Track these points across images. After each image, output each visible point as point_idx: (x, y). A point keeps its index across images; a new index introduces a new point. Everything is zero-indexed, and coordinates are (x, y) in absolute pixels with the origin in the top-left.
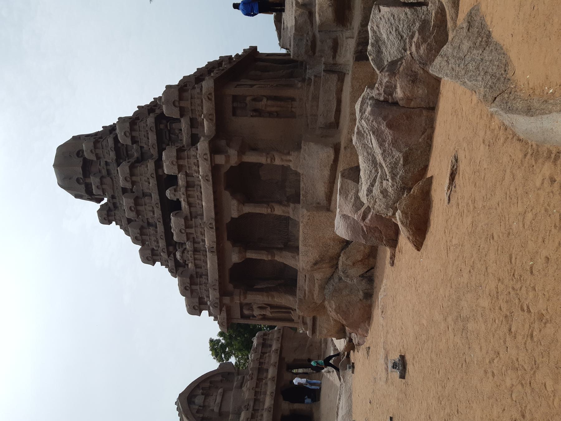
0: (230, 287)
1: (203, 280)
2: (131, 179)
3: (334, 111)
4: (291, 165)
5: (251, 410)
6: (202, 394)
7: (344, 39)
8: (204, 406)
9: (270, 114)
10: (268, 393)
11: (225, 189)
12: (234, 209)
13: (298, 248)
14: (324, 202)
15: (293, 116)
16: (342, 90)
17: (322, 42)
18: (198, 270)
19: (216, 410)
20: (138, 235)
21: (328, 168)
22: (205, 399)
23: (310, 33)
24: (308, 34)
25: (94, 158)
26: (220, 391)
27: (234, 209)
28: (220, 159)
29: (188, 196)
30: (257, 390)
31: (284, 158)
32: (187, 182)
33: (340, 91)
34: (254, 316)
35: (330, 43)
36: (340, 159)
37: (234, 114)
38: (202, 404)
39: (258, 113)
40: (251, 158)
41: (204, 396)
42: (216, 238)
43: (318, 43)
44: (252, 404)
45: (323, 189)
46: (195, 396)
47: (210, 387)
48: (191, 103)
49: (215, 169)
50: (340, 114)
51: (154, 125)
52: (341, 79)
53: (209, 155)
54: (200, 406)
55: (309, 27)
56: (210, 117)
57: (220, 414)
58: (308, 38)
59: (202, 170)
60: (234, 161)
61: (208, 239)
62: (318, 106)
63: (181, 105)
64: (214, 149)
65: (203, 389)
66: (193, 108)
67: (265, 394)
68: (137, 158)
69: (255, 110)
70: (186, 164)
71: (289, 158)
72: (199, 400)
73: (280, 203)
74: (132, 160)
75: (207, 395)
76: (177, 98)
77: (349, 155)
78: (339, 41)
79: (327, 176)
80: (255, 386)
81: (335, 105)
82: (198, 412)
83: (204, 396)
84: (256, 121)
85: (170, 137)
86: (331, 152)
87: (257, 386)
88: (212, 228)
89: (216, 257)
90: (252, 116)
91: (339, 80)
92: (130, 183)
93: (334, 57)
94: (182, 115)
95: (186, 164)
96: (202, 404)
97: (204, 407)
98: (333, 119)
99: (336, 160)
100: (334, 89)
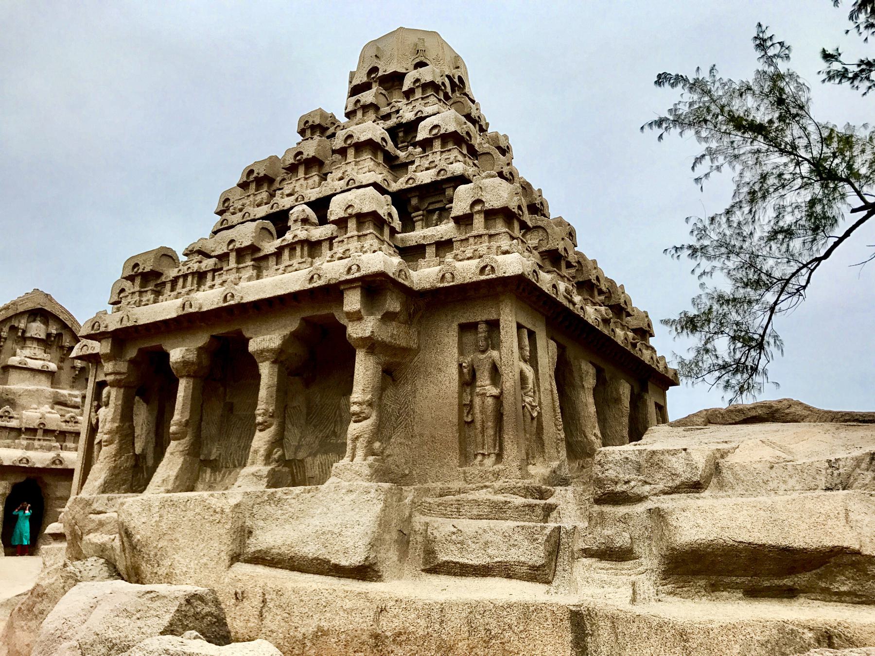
0: (132, 353)
1: (150, 296)
2: (350, 146)
3: (461, 561)
4: (346, 460)
6: (49, 335)
7: (633, 578)
10: (30, 454)
11: (303, 319)
12: (265, 340)
13: (192, 489)
14: (256, 544)
15: (465, 458)
16: (509, 577)
17: (625, 519)
18: (168, 286)
19: (14, 361)
20: (255, 175)
21: (323, 553)
22: (39, 340)
23: (647, 488)
24: (646, 483)
25: (405, 88)
26: (53, 366)
27: (265, 340)
28: (353, 301)
29: (292, 247)
30: (40, 432)
31: (361, 444)
33: (506, 571)
34: (99, 407)
35: (622, 540)
36: (343, 581)
37: (466, 328)
38: (28, 335)
39: (468, 380)
40: (364, 370)
41: (43, 336)
42: (208, 311)
43: (622, 510)
44: (14, 423)
45: (279, 542)
46: (46, 323)
47: (62, 347)
48: (480, 236)
49: (333, 292)
50: (455, 575)
51: (449, 175)
52: (538, 574)
53: (357, 275)
54: (24, 332)
55: (661, 486)
56: (448, 276)
57: (7, 368)
58: (632, 484)
59: (331, 268)
60: (356, 331)
62: (479, 517)
63: (476, 216)
64: (374, 286)
65: (59, 336)
66: (471, 240)
67: (27, 448)
68: (397, 157)
69: (473, 373)
70: (349, 235)
71: (360, 453)
72: (37, 329)
73: (278, 441)
74: (390, 146)
75: (46, 343)
76: (488, 206)
77: (348, 604)
78: (629, 564)
79: (306, 550)
80: (48, 427)
81: (475, 562)
82: (13, 329)
83: (43, 336)
85: (432, 212)
86: (355, 559)
87: (47, 432)
88: (225, 299)
89: (174, 315)
90: (460, 365)
91: (533, 568)
92: (343, 145)
93: (588, 553)
94: (458, 220)
95: (349, 235)
96: (28, 335)
97: (23, 339)
98: (443, 557)
99: (339, 571)
100: (513, 556)
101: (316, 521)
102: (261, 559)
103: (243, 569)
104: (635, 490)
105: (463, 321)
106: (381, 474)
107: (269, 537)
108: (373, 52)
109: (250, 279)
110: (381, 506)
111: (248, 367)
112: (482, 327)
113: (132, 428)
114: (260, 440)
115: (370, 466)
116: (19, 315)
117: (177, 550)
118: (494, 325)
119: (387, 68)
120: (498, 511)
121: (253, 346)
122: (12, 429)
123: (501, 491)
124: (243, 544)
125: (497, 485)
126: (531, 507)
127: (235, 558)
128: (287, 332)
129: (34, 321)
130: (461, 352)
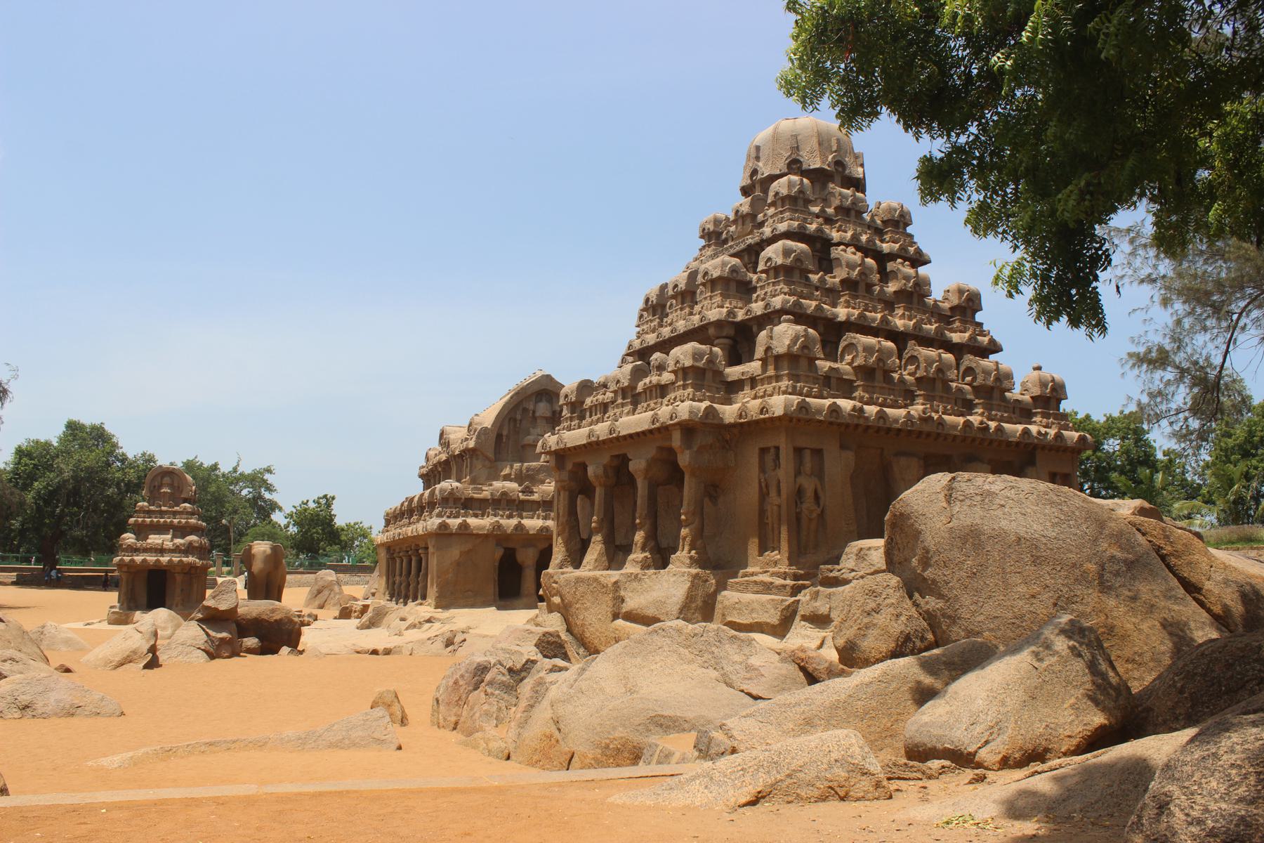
0: (569, 466)
5: (522, 497)
8: (534, 418)
9: (762, 512)
14: (626, 607)
17: (829, 596)
24: (853, 570)
32: (666, 385)
35: (823, 610)
37: (763, 451)
40: (689, 488)
44: (536, 497)
49: (664, 430)
54: (534, 412)
60: (684, 459)
61: (601, 429)
62: (757, 592)
64: (688, 429)
67: (545, 518)
71: (687, 548)
82: (525, 410)
84: (753, 492)
89: (585, 442)
93: (804, 618)
96: (537, 414)
98: (729, 619)
101: (655, 594)
102: (631, 617)
103: (620, 622)
104: (845, 576)
105: (762, 446)
106: (694, 562)
107: (633, 602)
108: (753, 155)
109: (628, 414)
110: (689, 584)
111: (632, 480)
112: (772, 450)
113: (577, 520)
114: (639, 536)
115: (691, 558)
116: (528, 398)
117: (586, 609)
118: (777, 448)
119: (765, 170)
120: (767, 588)
121: (633, 466)
122: (533, 502)
123: (773, 574)
124: (619, 608)
125: (776, 569)
126: (784, 586)
127: (616, 616)
128: (649, 456)
129: (541, 401)
130: (762, 469)
